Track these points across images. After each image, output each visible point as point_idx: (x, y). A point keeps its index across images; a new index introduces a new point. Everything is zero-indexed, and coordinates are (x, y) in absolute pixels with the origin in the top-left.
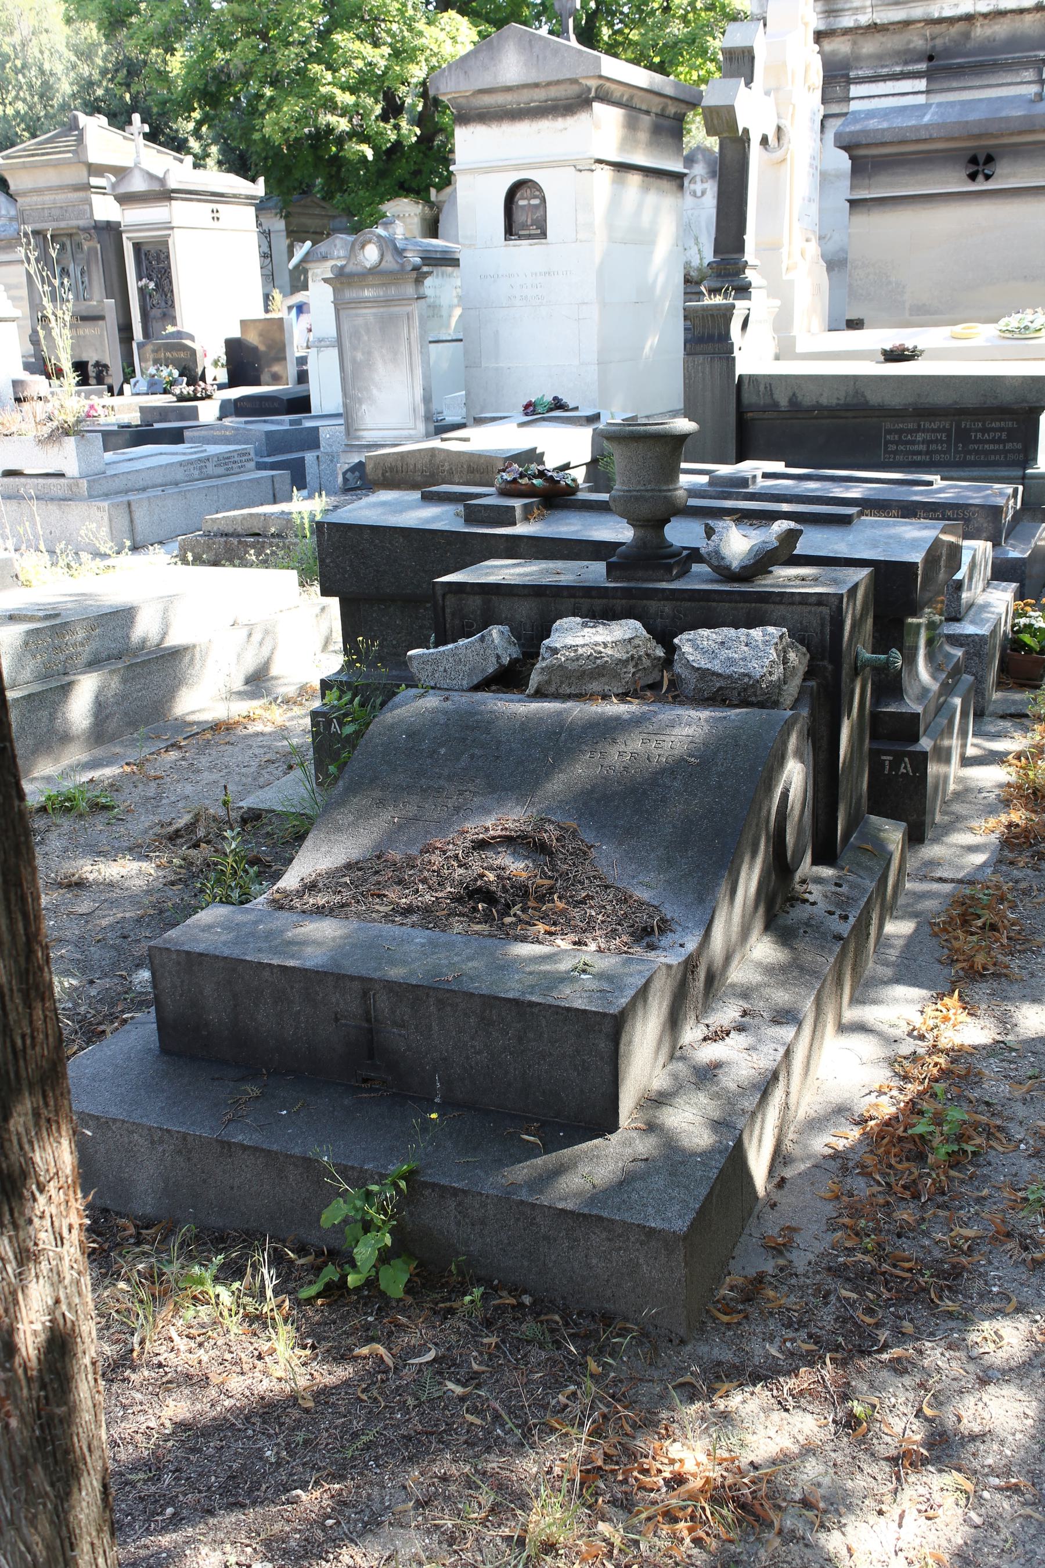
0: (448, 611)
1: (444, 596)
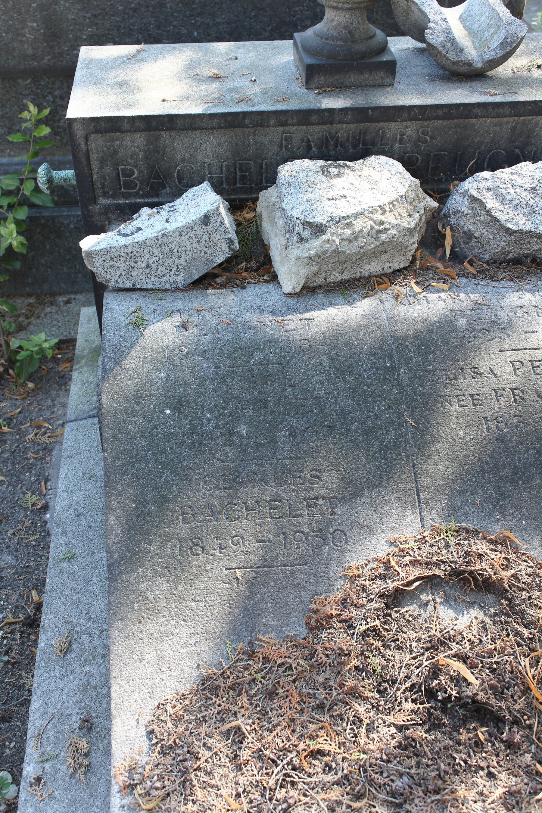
0: (94, 156)
1: (86, 138)
